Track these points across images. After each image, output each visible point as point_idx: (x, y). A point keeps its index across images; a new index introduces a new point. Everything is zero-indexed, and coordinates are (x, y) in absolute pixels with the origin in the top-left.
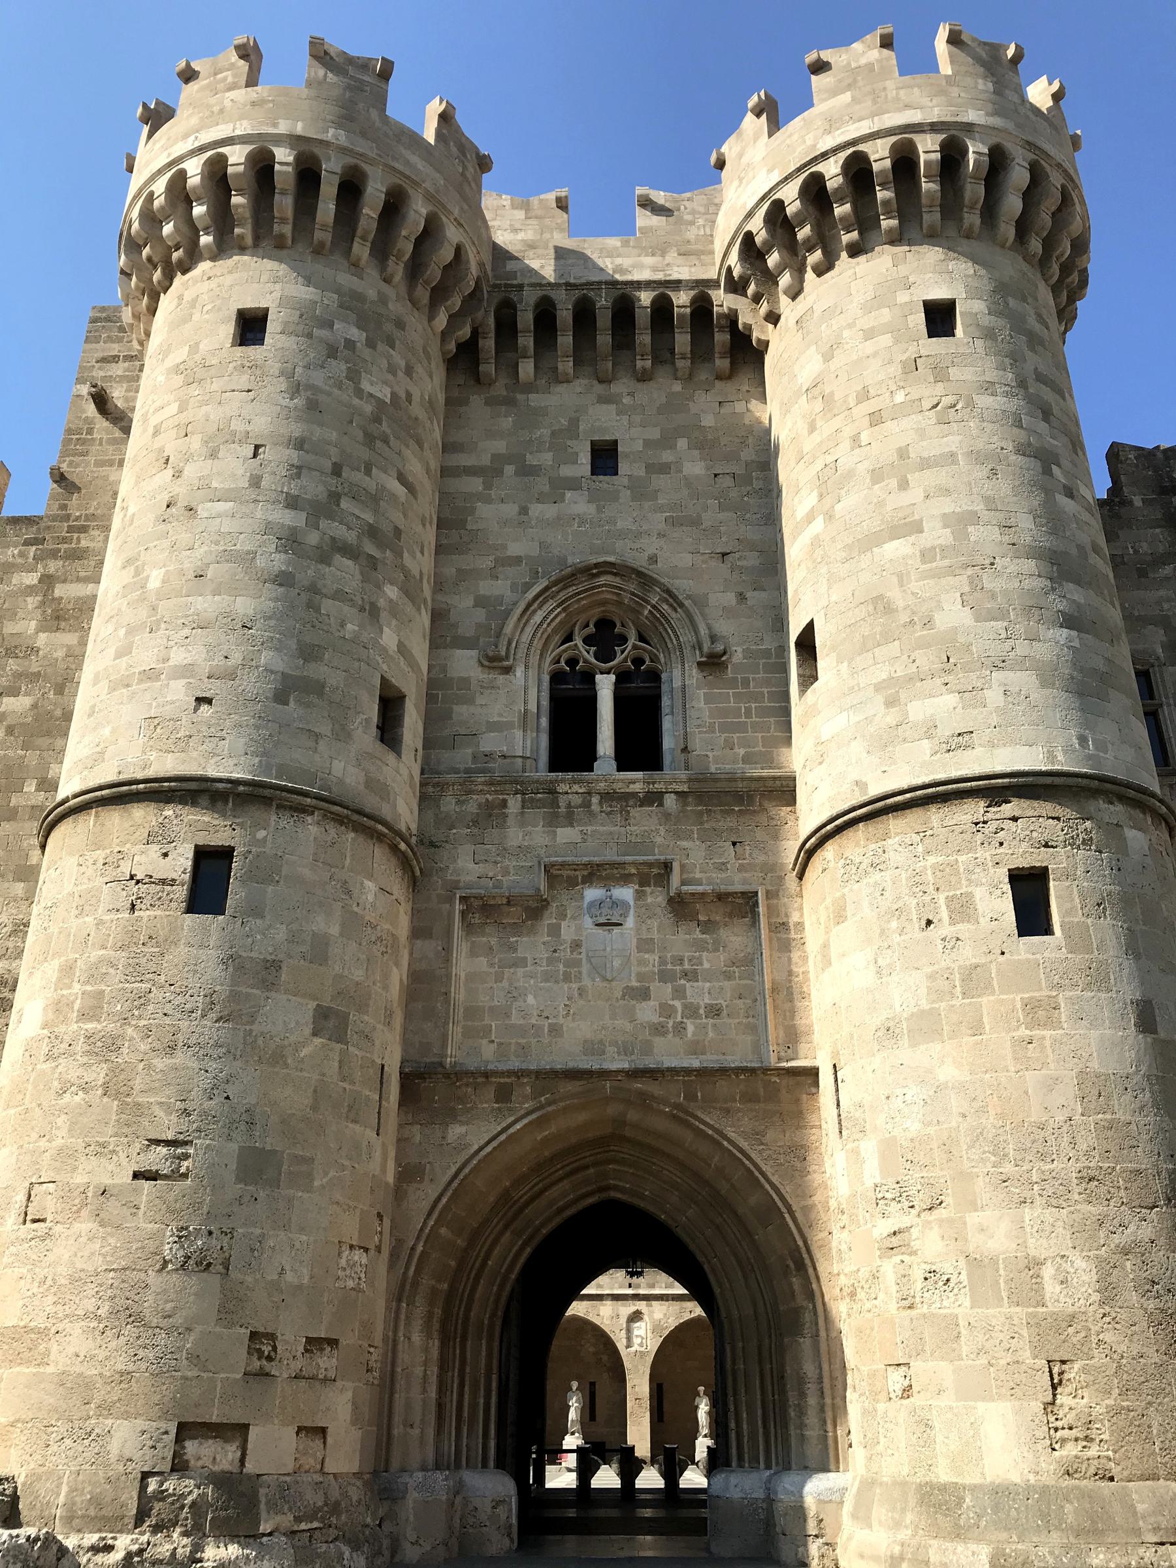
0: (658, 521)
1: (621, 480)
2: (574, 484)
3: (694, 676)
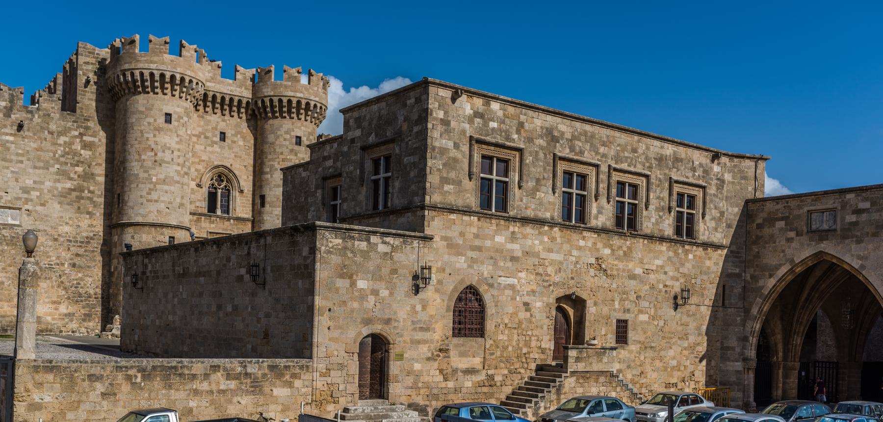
0: (233, 155)
1: (226, 144)
2: (216, 143)
3: (238, 194)
